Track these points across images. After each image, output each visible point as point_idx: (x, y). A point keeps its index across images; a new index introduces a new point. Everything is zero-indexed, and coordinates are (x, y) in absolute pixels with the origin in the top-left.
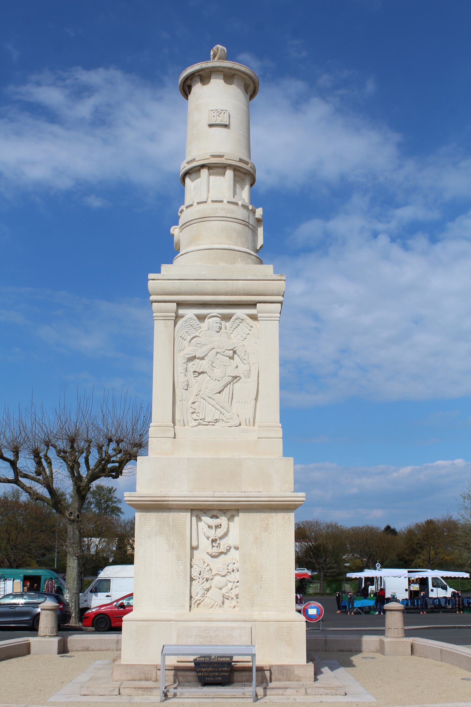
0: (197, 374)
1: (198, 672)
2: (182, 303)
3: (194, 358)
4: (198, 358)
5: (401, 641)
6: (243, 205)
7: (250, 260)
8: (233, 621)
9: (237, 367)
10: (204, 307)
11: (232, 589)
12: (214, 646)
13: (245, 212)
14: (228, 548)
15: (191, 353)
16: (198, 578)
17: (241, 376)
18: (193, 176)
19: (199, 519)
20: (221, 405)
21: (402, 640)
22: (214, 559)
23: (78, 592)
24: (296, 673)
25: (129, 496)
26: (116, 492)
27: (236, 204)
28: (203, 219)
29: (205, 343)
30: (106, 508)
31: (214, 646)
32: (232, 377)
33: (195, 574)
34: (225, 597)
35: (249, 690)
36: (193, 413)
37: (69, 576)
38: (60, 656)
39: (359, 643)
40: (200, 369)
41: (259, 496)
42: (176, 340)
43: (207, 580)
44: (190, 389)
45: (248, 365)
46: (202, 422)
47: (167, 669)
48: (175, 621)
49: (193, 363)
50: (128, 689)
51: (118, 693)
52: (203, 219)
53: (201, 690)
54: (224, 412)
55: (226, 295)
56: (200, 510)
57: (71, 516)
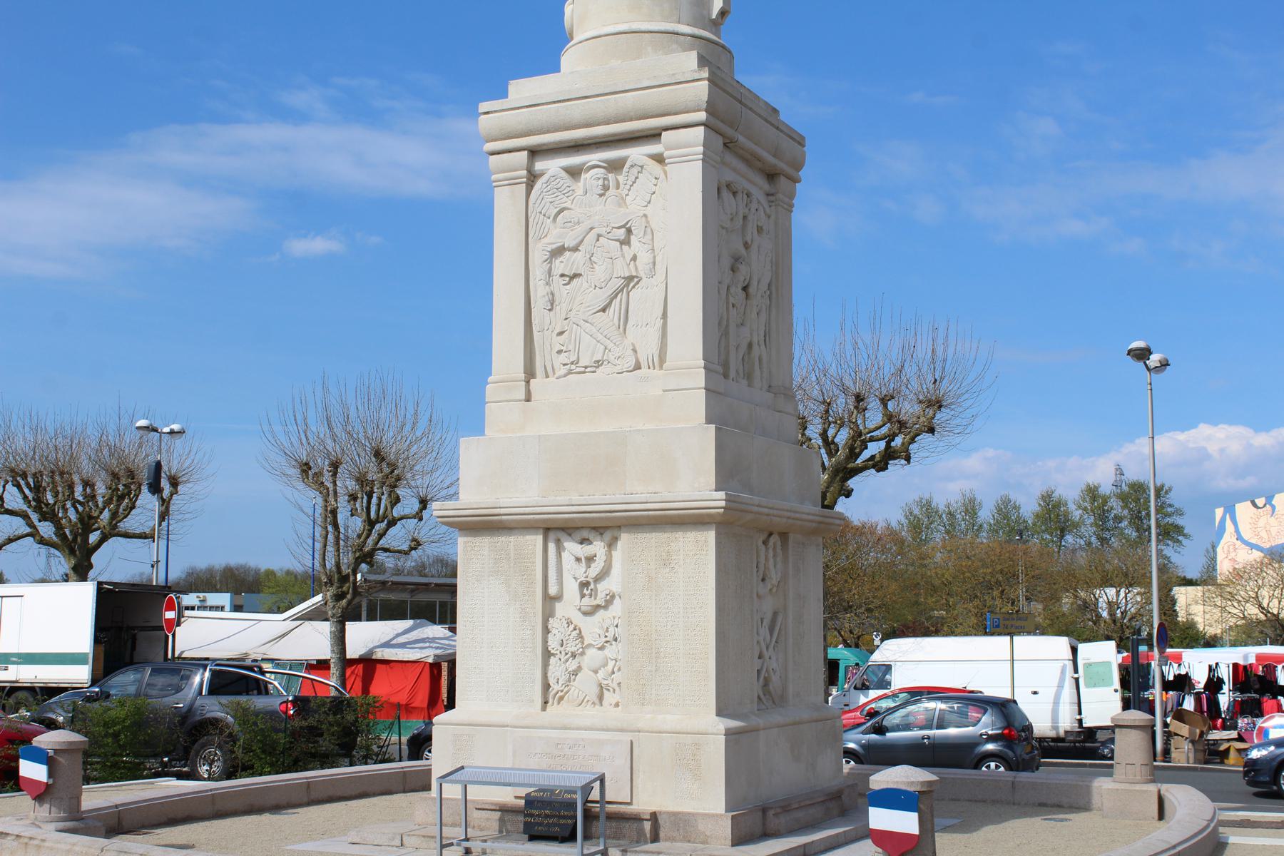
0: (567, 279)
1: (526, 816)
2: (539, 149)
4: (570, 249)
5: (1138, 791)
7: (675, 46)
8: (603, 730)
10: (578, 151)
11: (613, 673)
12: (571, 772)
14: (608, 597)
15: (554, 241)
16: (558, 652)
17: (642, 274)
20: (604, 334)
21: (1138, 787)
22: (588, 618)
24: (699, 828)
25: (439, 508)
26: (1171, 494)
29: (579, 220)
31: (571, 772)
32: (623, 278)
38: (1042, 819)
39: (1088, 791)
40: (571, 269)
41: (645, 501)
42: (531, 220)
43: (574, 656)
45: (651, 253)
46: (574, 368)
47: (480, 807)
48: (511, 727)
49: (561, 259)
50: (413, 838)
51: (399, 844)
53: (521, 846)
54: (610, 345)
55: (608, 124)
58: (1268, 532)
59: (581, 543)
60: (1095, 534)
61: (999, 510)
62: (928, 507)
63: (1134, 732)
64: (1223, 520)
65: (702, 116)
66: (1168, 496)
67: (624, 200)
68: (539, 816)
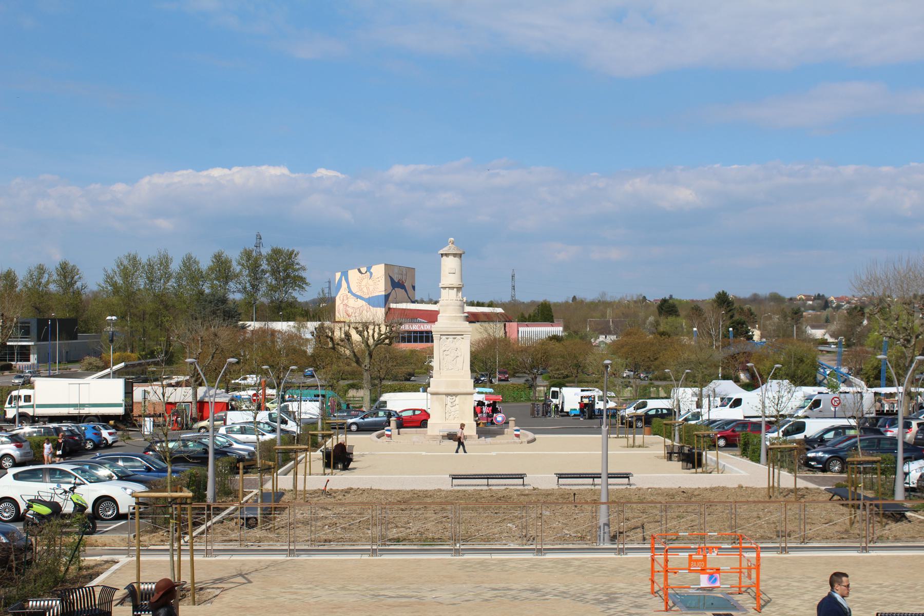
13: (460, 302)
26: (299, 257)
28: (447, 305)
30: (284, 279)
34: (455, 418)
52: (447, 305)
58: (368, 289)
60: (249, 281)
61: (184, 264)
62: (134, 260)
64: (340, 280)
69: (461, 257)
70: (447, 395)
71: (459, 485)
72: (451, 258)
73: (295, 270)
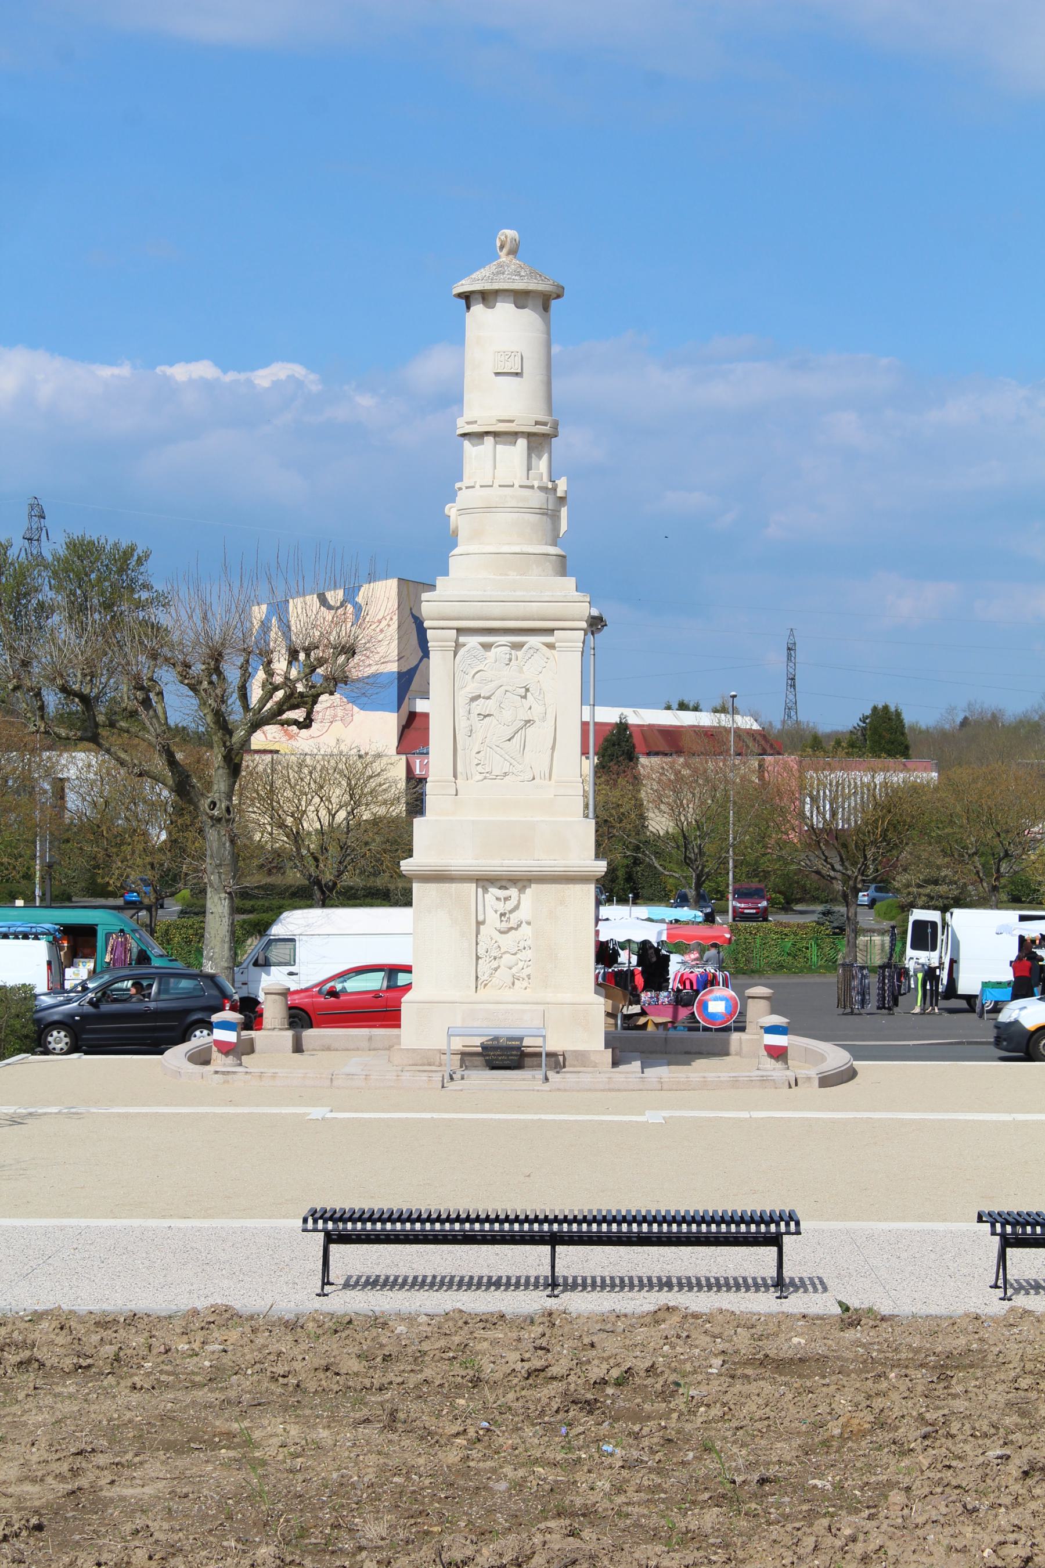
3: (479, 696)
4: (484, 698)
6: (539, 487)
9: (530, 708)
13: (543, 494)
17: (536, 719)
18: (476, 441)
19: (485, 890)
23: (231, 965)
26: (149, 566)
27: (532, 487)
28: (488, 509)
33: (481, 952)
34: (515, 979)
35: (539, 1074)
36: (478, 765)
37: (213, 932)
43: (495, 958)
44: (474, 735)
49: (477, 703)
52: (488, 509)
54: (515, 763)
56: (487, 880)
57: (213, 809)
59: (500, 889)
63: (763, 1001)
65: (584, 625)
66: (142, 569)
67: (522, 668)
68: (494, 1055)
69: (546, 308)
70: (485, 881)
71: (373, 1283)
72: (505, 309)
73: (140, 605)
